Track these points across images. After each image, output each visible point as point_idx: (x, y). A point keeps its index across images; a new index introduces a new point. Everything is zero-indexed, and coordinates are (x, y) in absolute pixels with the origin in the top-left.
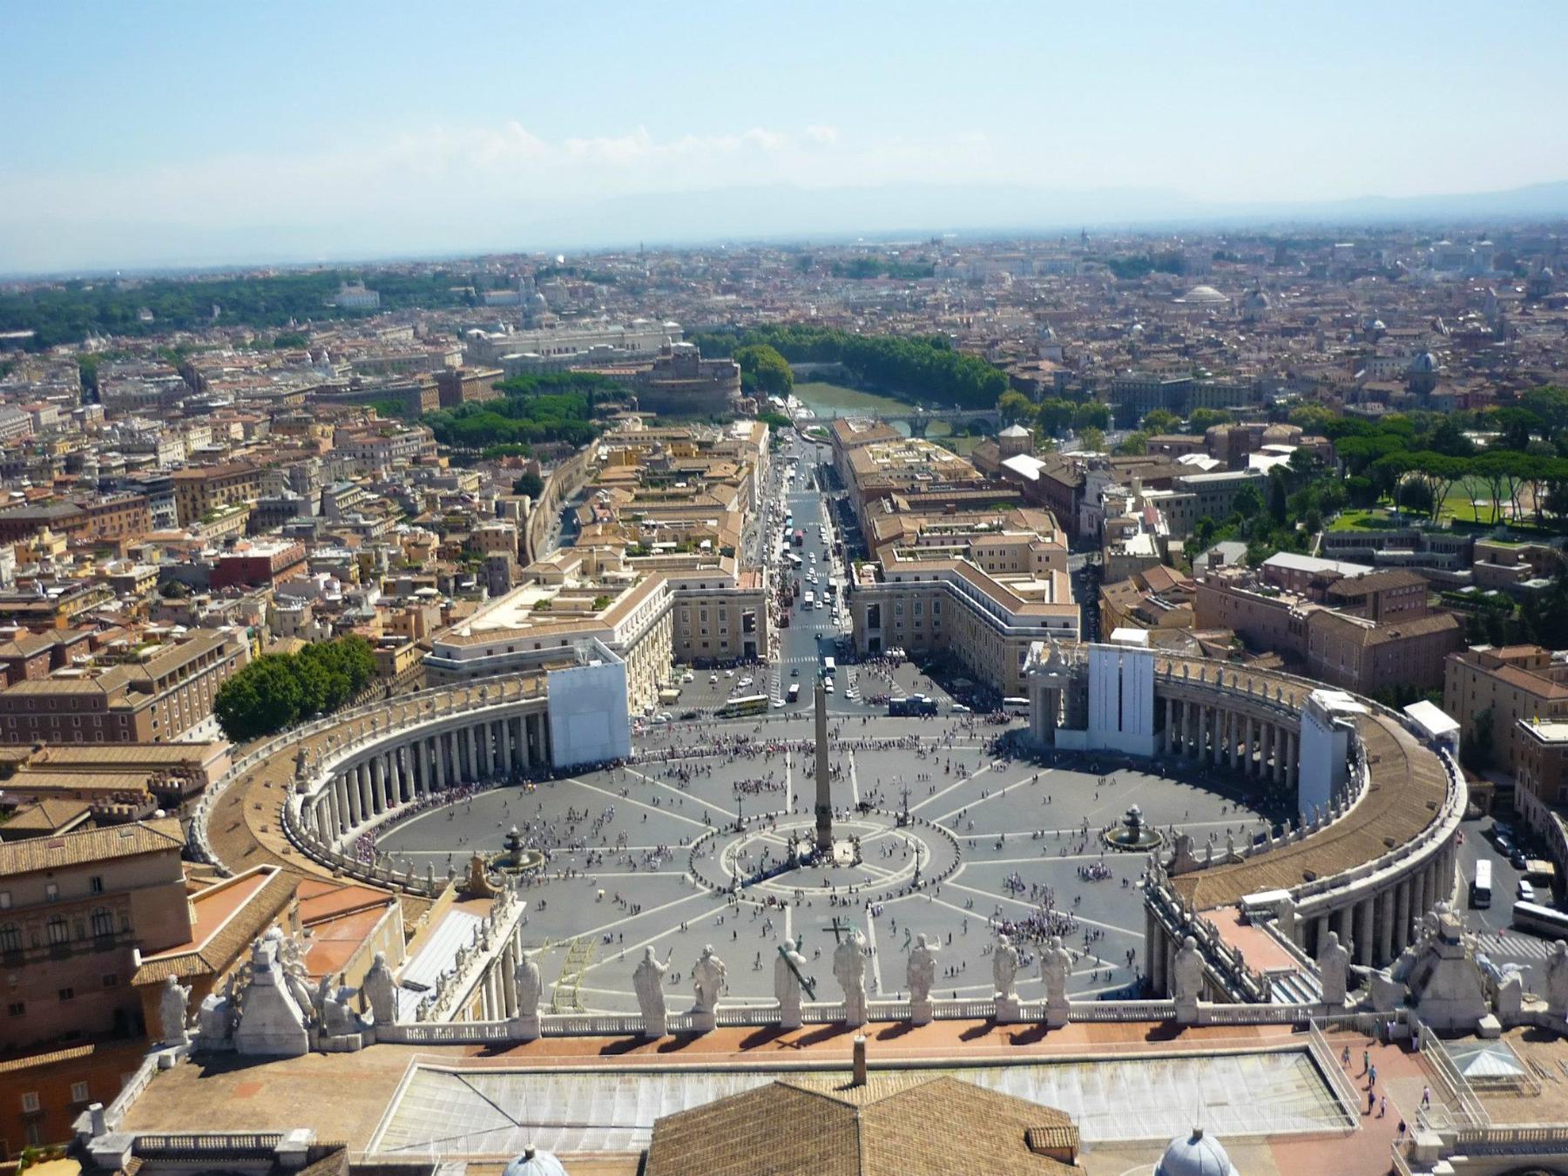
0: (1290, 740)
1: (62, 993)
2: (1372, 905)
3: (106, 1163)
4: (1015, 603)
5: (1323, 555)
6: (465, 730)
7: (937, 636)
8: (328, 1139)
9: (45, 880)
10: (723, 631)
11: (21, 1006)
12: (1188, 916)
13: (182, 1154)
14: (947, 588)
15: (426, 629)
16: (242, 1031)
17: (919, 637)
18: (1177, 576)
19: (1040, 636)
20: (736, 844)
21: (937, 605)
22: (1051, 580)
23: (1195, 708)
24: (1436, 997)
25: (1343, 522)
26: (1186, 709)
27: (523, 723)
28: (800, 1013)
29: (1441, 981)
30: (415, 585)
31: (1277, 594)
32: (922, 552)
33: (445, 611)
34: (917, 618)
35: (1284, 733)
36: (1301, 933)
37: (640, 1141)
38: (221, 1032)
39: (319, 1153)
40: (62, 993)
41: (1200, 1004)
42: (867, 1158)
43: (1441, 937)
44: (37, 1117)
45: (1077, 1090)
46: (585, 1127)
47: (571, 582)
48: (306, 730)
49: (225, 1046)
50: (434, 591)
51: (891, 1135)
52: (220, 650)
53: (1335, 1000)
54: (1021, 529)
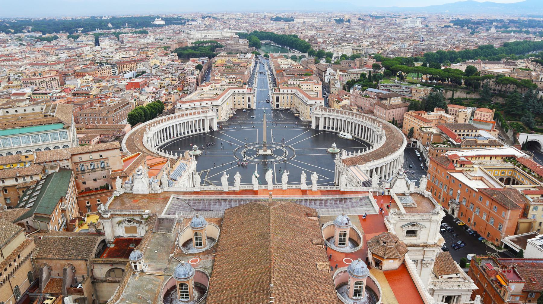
1: (94, 180)
2: (384, 167)
3: (105, 216)
5: (378, 89)
8: (153, 212)
9: (89, 155)
11: (85, 182)
13: (120, 215)
16: (134, 188)
18: (346, 92)
20: (245, 150)
24: (396, 186)
25: (383, 83)
29: (397, 183)
35: (368, 128)
36: (369, 172)
37: (221, 214)
38: (129, 189)
39: (151, 215)
40: (94, 180)
42: (271, 218)
43: (399, 174)
44: (90, 206)
45: (318, 204)
46: (210, 211)
48: (147, 123)
49: (130, 192)
51: (277, 214)
52: (128, 104)
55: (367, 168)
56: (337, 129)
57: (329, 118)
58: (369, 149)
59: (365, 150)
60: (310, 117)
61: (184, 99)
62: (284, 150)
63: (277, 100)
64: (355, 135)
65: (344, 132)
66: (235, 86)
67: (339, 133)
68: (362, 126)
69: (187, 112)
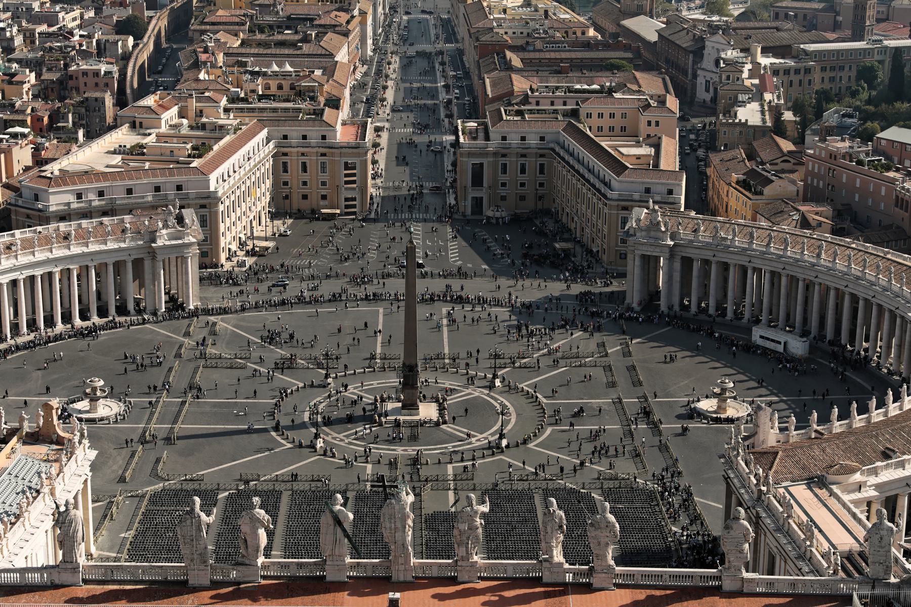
0: (887, 315)
4: (618, 167)
6: (50, 274)
7: (540, 198)
10: (324, 184)
12: (764, 489)
14: (553, 150)
15: (17, 169)
17: (523, 198)
18: (787, 146)
19: (643, 203)
21: (542, 165)
22: (657, 147)
23: (793, 280)
26: (784, 280)
27: (111, 269)
28: (343, 567)
30: (8, 124)
31: (888, 169)
32: (531, 112)
33: (37, 149)
34: (522, 178)
41: (746, 575)
47: (164, 129)
50: (26, 131)
53: (881, 575)
54: (634, 92)
55: (872, 493)
56: (738, 315)
57: (706, 263)
58: (881, 404)
59: (863, 409)
60: (623, 256)
61: (54, 168)
62: (499, 400)
63: (477, 180)
64: (821, 337)
65: (772, 324)
66: (291, 114)
67: (749, 332)
68: (855, 299)
69: (63, 226)
